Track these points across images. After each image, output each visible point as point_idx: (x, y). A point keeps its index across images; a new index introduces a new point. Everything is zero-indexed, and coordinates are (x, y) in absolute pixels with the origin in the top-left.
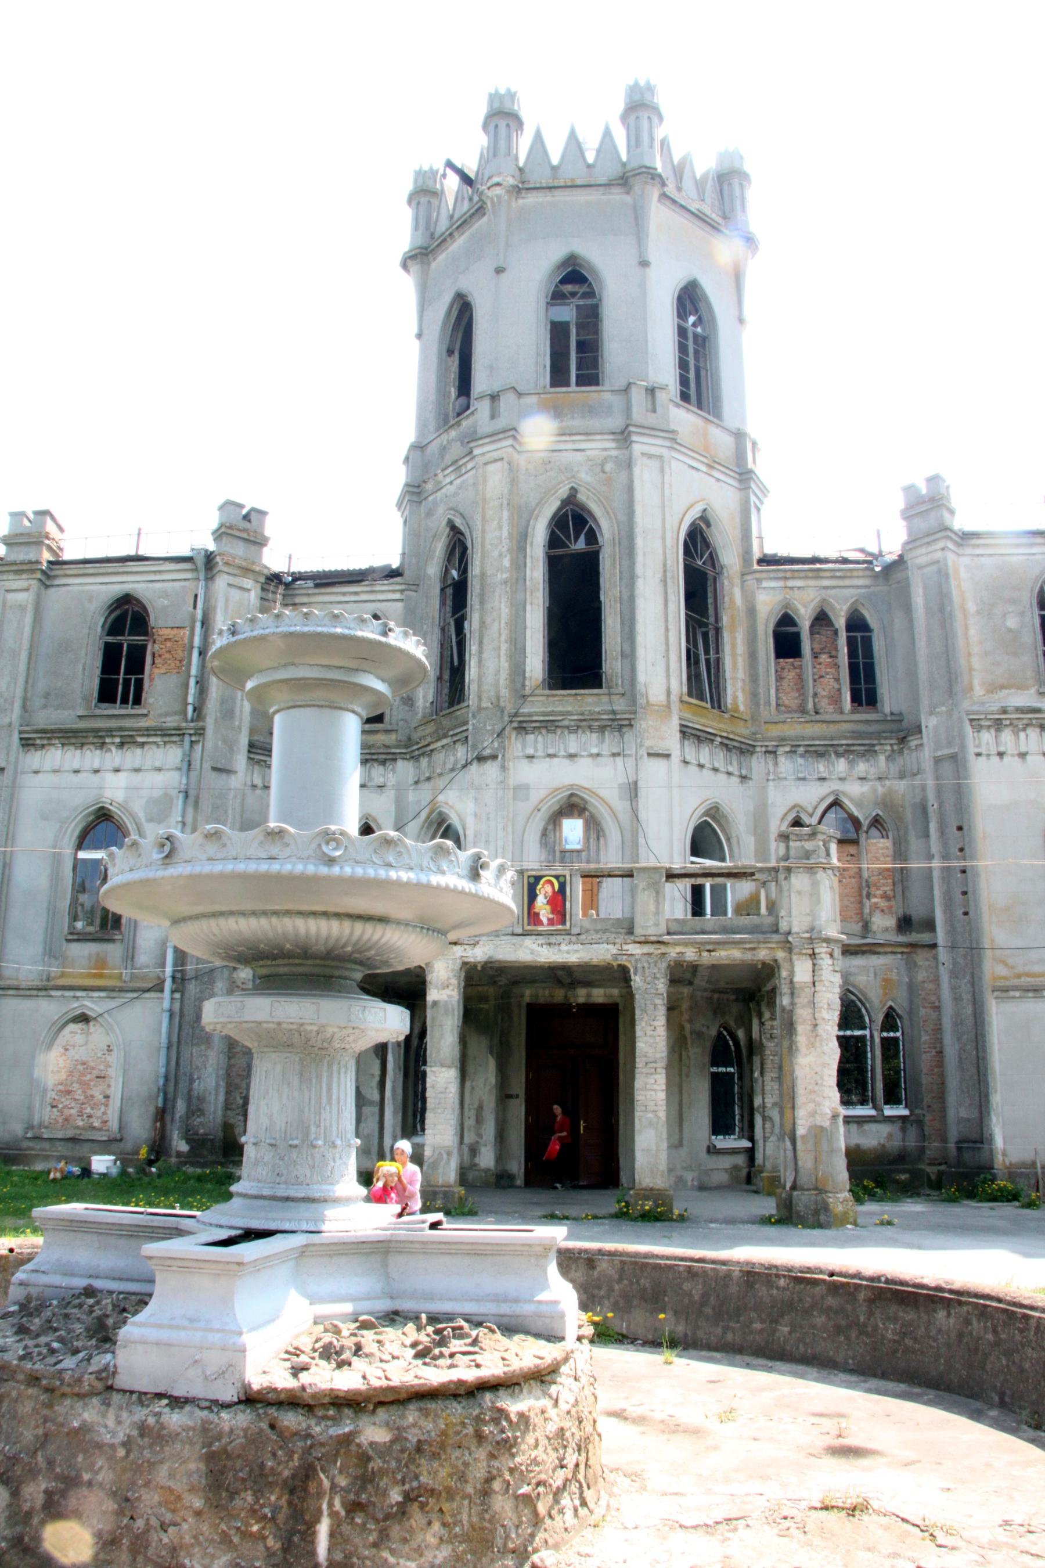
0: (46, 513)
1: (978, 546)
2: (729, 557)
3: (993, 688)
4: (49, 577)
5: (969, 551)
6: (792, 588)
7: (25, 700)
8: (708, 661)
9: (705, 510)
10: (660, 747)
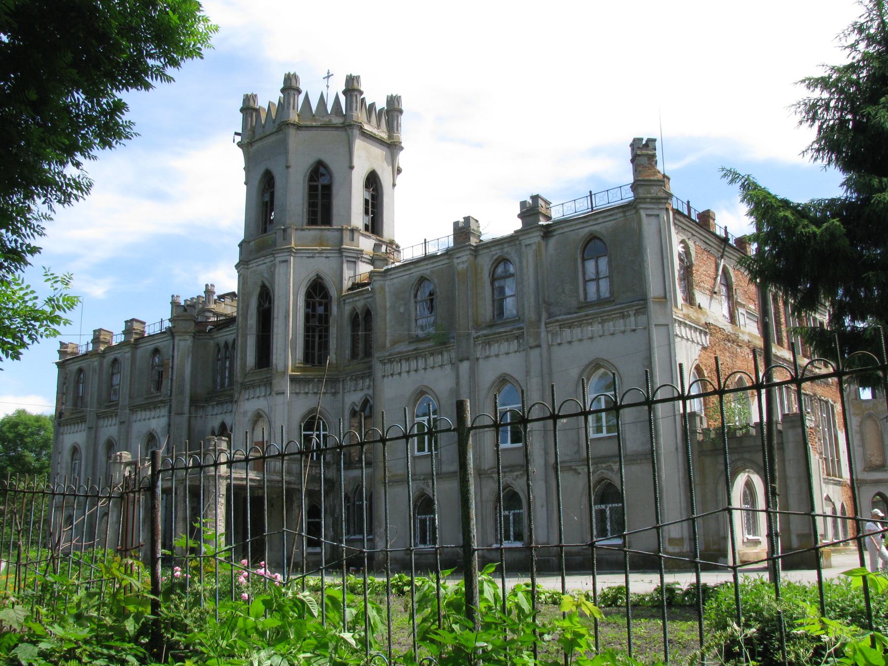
0: (133, 320)
1: (391, 274)
2: (333, 293)
3: (394, 343)
4: (137, 345)
5: (389, 277)
7: (130, 394)
8: (320, 344)
9: (317, 274)
10: (280, 389)
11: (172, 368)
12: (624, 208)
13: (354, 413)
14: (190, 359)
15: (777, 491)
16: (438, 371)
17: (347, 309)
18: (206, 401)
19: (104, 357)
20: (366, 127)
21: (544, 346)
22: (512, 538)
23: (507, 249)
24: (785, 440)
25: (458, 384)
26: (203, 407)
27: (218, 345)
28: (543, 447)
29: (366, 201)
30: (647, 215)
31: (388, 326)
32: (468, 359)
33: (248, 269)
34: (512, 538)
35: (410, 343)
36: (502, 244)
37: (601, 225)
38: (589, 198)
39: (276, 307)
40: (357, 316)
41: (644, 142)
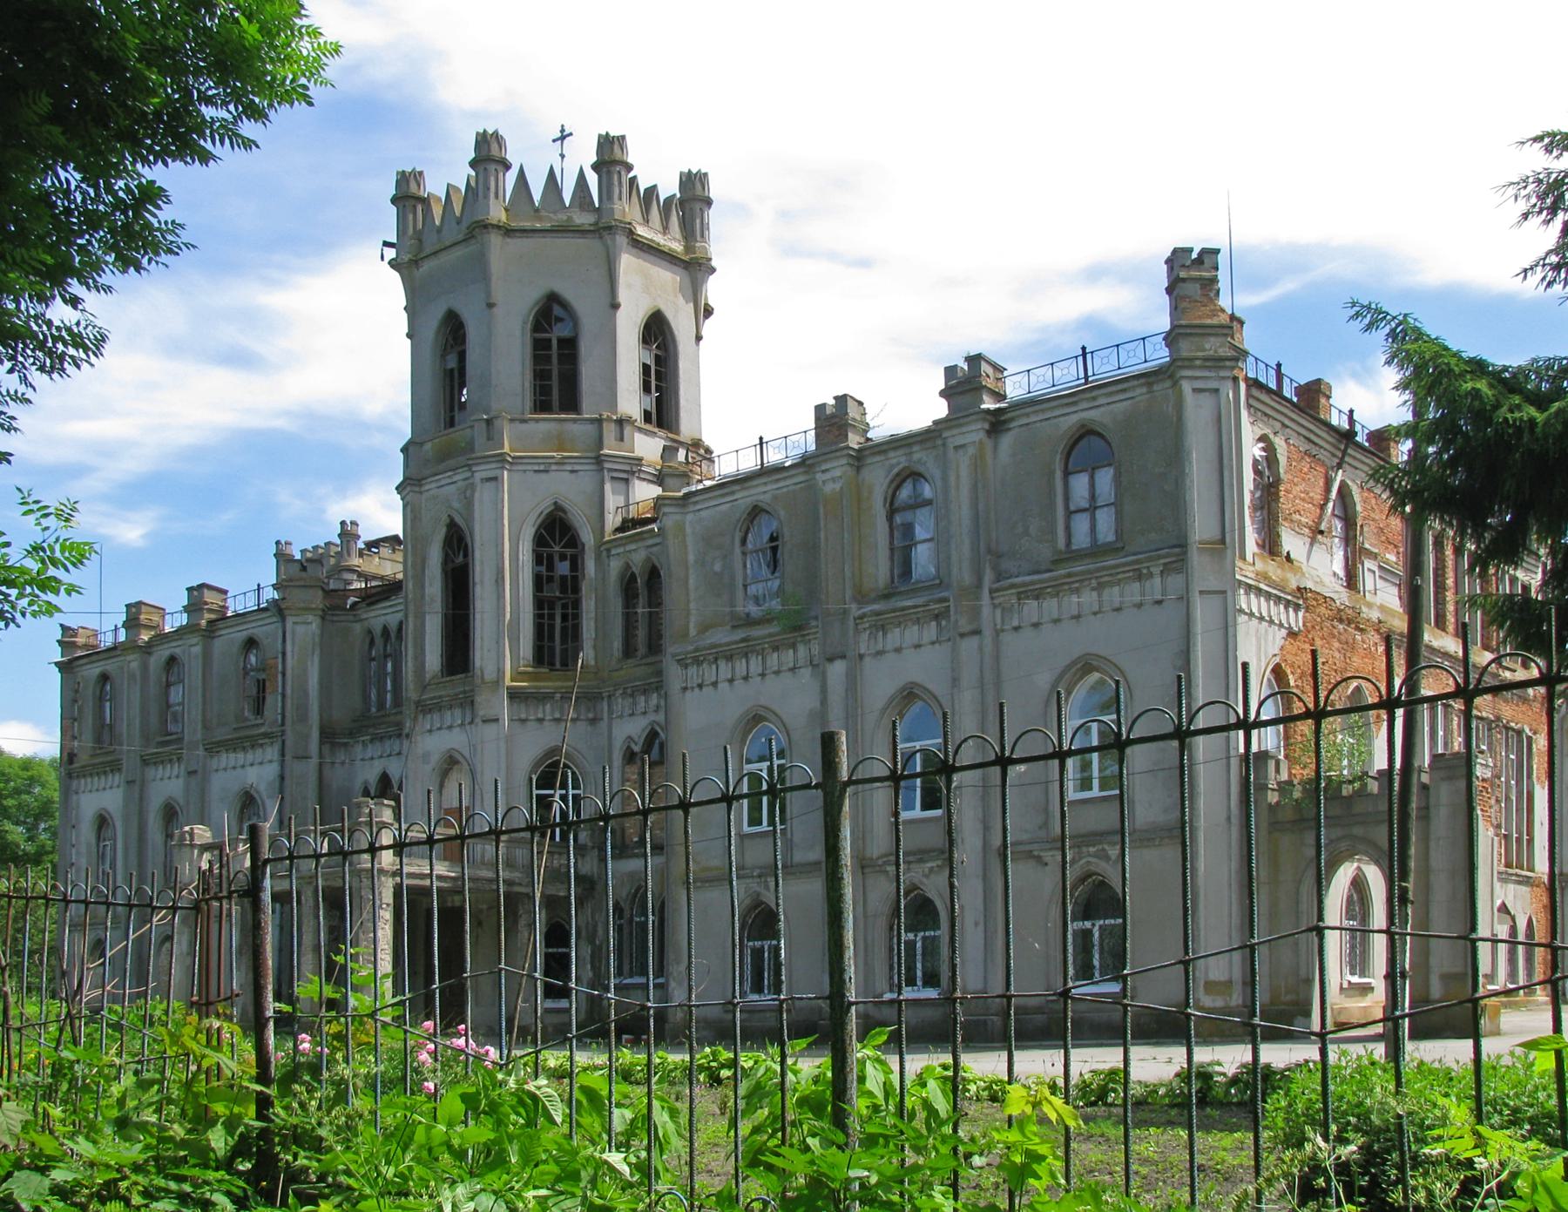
0: (202, 586)
1: (696, 502)
2: (587, 537)
3: (704, 628)
4: (213, 631)
5: (692, 508)
6: (630, 551)
7: (204, 721)
8: (564, 630)
9: (555, 503)
10: (491, 714)
11: (284, 674)
12: (1148, 378)
13: (630, 757)
14: (316, 659)
15: (1411, 896)
16: (786, 677)
17: (615, 566)
18: (351, 734)
19: (150, 654)
20: (641, 231)
21: (988, 632)
22: (919, 983)
23: (919, 454)
24: (1432, 801)
25: (824, 701)
26: (345, 745)
27: (370, 632)
28: (980, 816)
29: (646, 369)
30: (1194, 390)
31: (692, 595)
32: (843, 657)
33: (421, 493)
34: (919, 983)
35: (734, 627)
36: (910, 445)
37: (1102, 409)
38: (1080, 359)
39: (477, 563)
40: (633, 577)
41: (1194, 255)
